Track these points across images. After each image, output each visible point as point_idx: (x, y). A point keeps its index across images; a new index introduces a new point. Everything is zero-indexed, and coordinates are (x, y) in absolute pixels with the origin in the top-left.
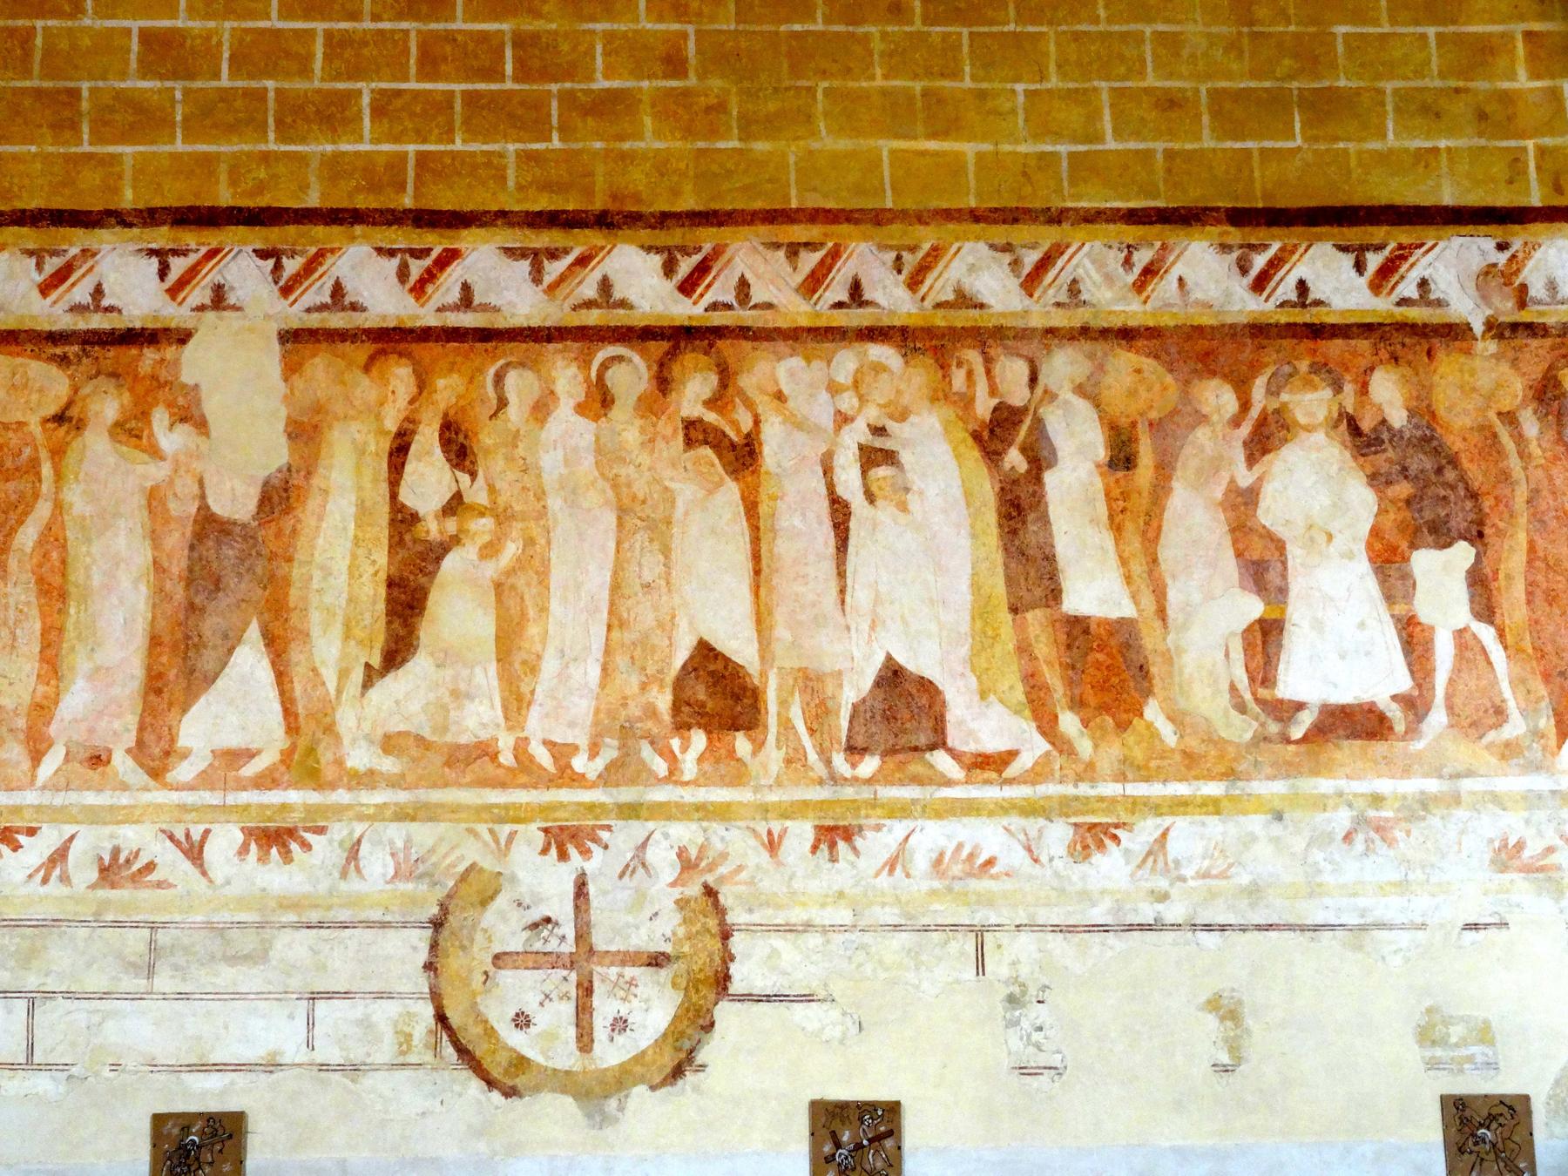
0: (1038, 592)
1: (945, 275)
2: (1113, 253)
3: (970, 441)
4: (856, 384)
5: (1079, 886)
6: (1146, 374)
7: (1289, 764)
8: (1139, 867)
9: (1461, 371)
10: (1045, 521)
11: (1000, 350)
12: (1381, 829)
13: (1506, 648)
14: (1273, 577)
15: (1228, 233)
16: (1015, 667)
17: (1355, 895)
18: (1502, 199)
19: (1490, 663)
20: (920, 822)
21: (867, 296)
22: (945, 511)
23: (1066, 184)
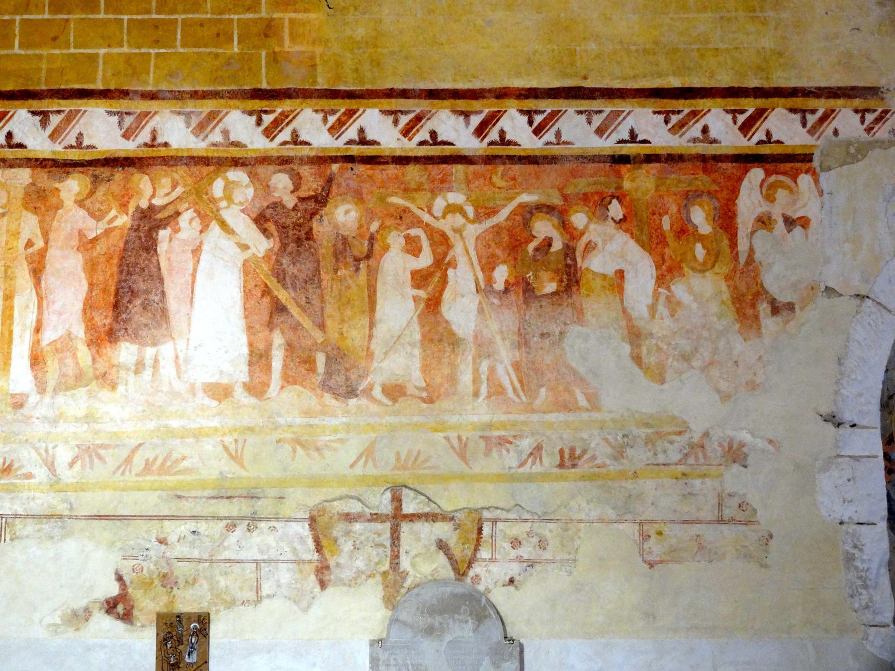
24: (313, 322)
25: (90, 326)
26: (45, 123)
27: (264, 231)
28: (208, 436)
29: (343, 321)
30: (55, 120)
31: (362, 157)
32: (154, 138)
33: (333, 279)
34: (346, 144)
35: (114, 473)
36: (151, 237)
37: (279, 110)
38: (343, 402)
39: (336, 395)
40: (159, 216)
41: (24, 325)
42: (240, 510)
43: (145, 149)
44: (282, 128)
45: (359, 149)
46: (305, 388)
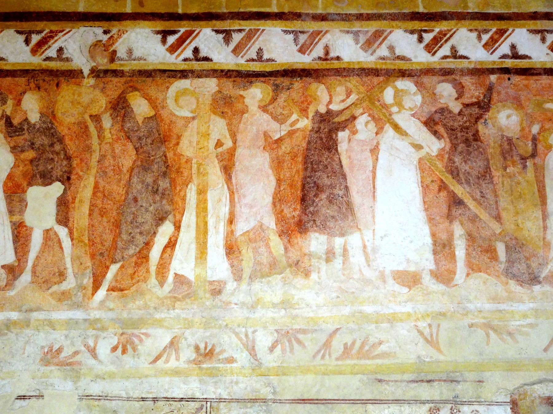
9: (73, 94)
13: (72, 240)
18: (111, 9)
19: (61, 248)
24: (489, 214)
25: (280, 218)
26: (228, 40)
27: (435, 133)
28: (401, 321)
29: (517, 213)
30: (237, 38)
31: (517, 69)
32: (327, 53)
33: (503, 176)
34: (500, 58)
35: (314, 357)
36: (331, 138)
37: (437, 30)
38: (528, 289)
39: (521, 282)
40: (336, 120)
41: (218, 216)
42: (441, 393)
43: (320, 62)
44: (442, 45)
45: (514, 62)
46: (489, 275)
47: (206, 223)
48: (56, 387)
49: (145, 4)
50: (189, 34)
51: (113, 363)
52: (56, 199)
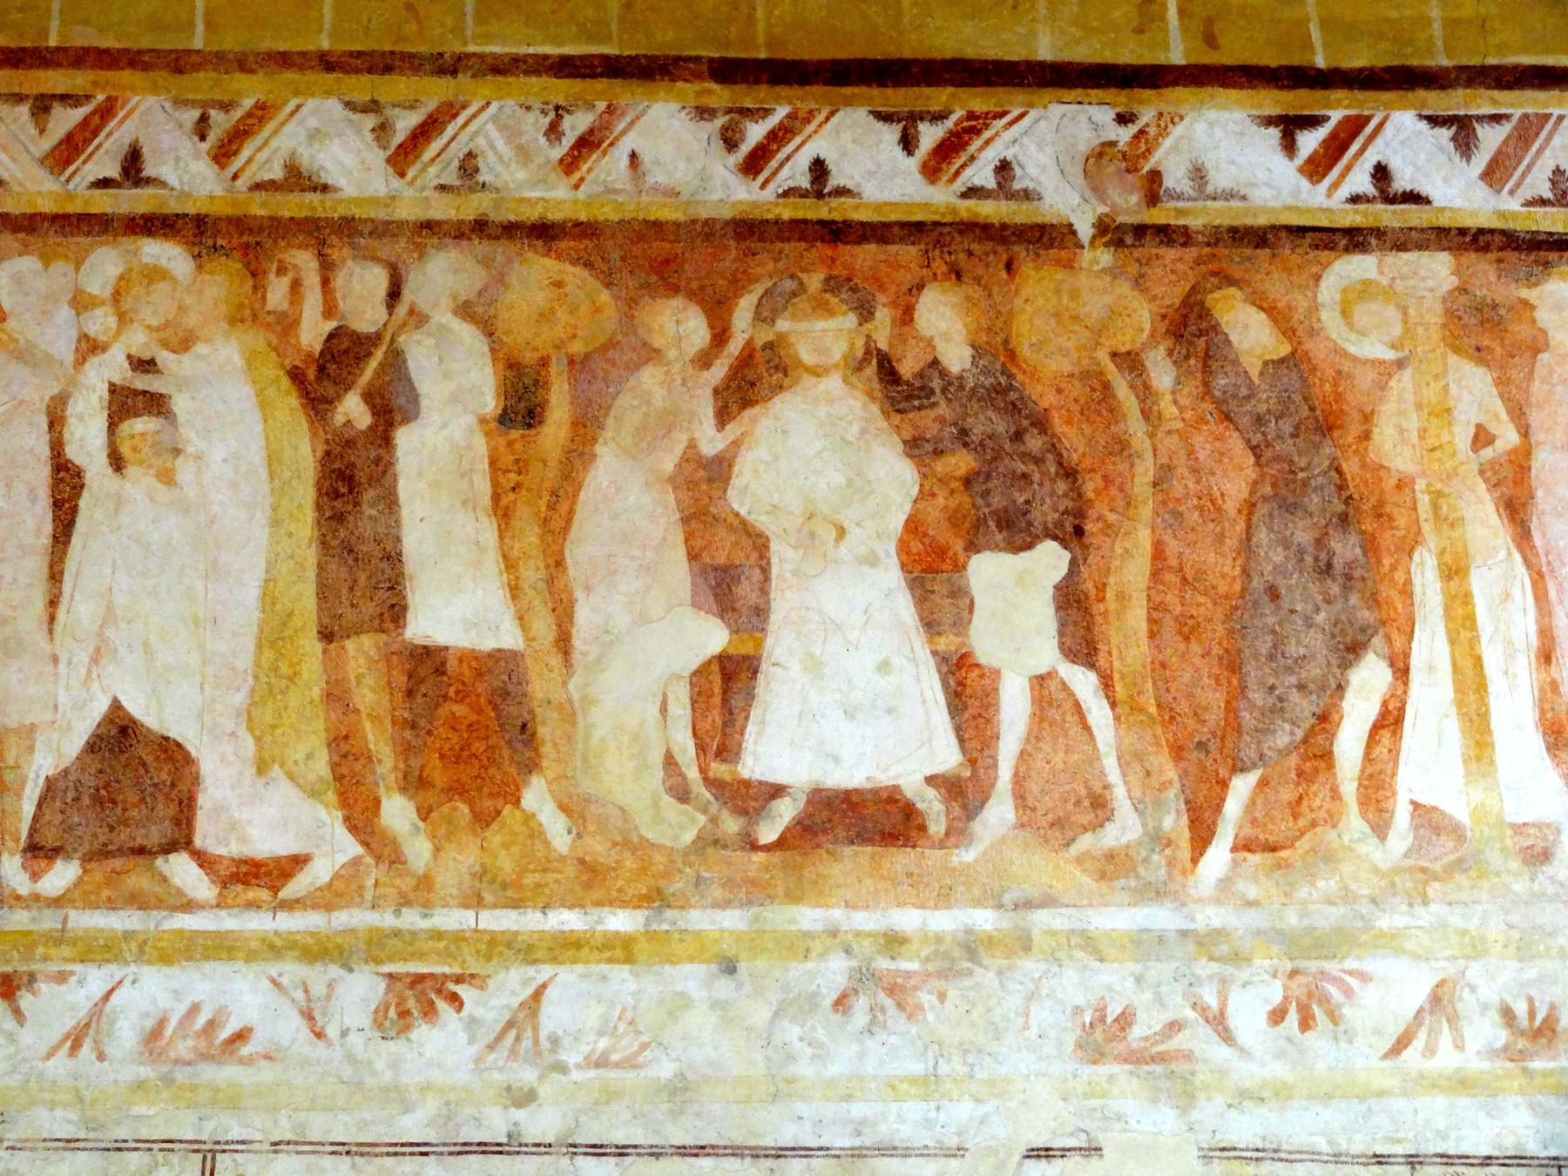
0: (369, 609)
1: (274, 144)
2: (531, 117)
3: (285, 382)
4: (117, 295)
5: (387, 1076)
6: (569, 289)
7: (753, 882)
8: (491, 1047)
9: (1057, 292)
10: (391, 502)
11: (346, 251)
12: (897, 990)
13: (1113, 705)
14: (746, 591)
15: (710, 92)
16: (320, 724)
17: (848, 1098)
18: (1127, 53)
19: (1087, 728)
20: (133, 968)
21: (149, 171)
22: (234, 485)
23: (469, 20)
26: (1467, 145)
30: (1491, 138)
41: (1509, 642)
47: (1478, 662)
48: (1133, 1124)
49: (1222, 41)
50: (1353, 127)
51: (1280, 1055)
52: (1051, 591)
